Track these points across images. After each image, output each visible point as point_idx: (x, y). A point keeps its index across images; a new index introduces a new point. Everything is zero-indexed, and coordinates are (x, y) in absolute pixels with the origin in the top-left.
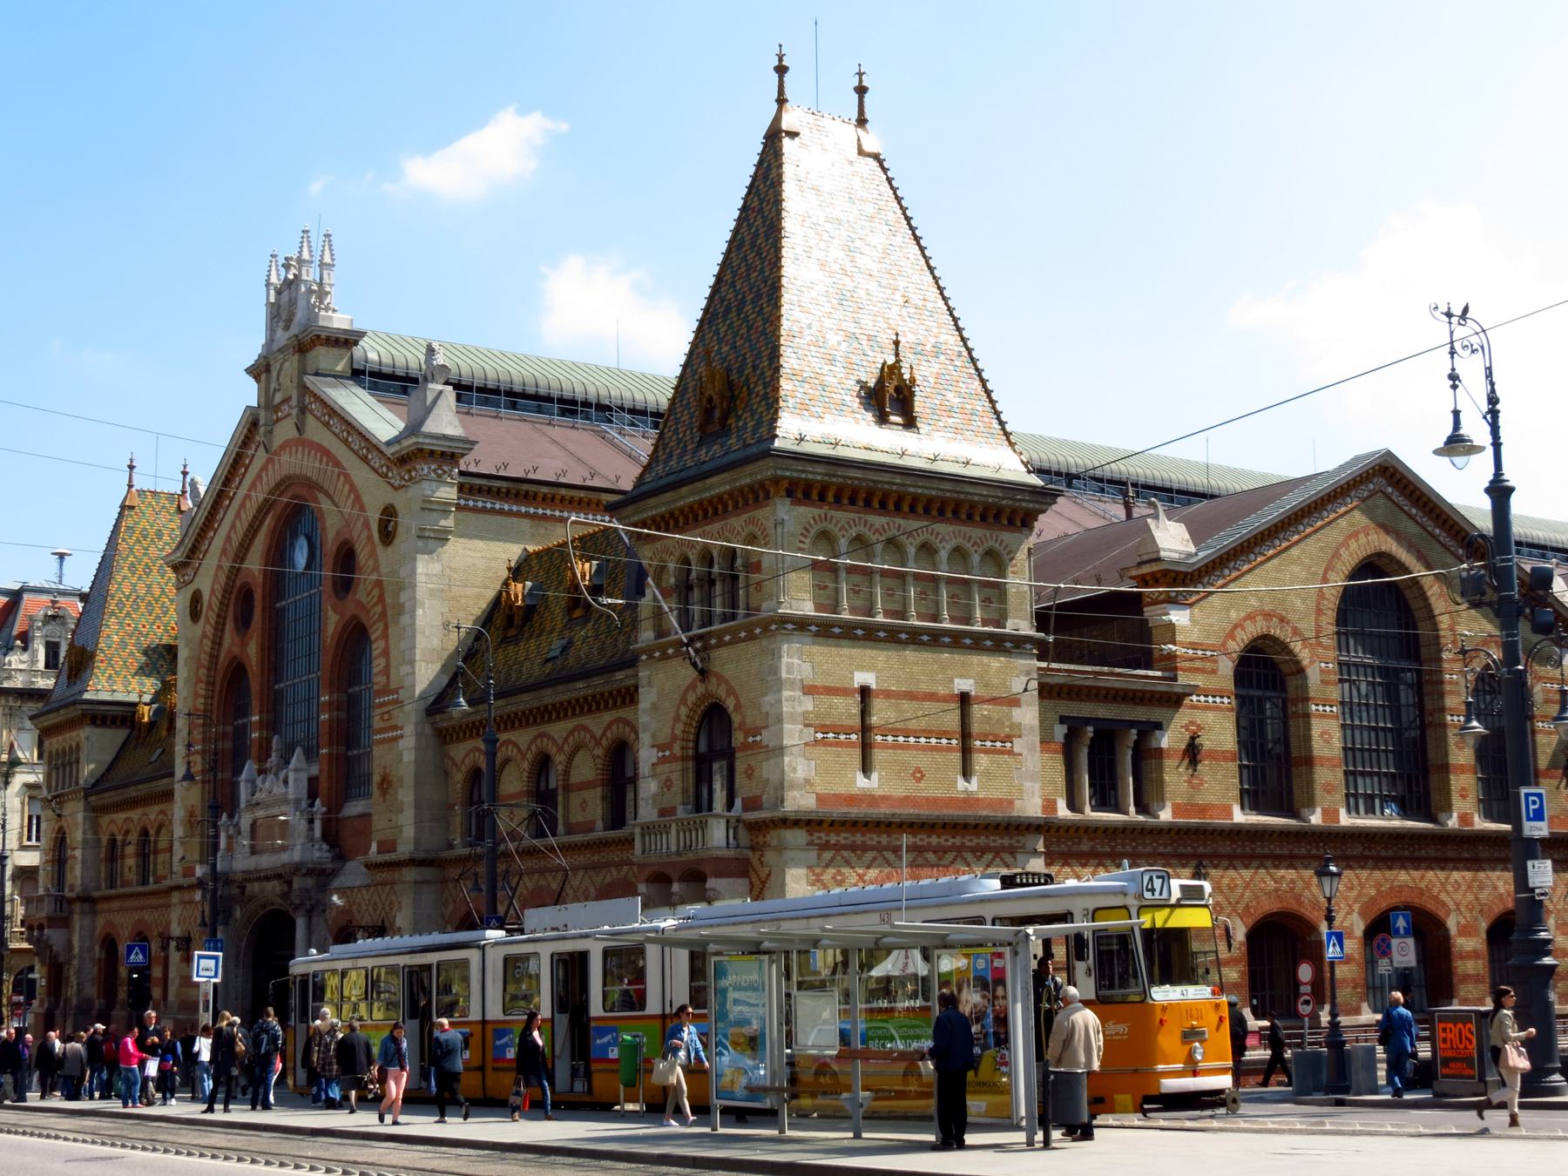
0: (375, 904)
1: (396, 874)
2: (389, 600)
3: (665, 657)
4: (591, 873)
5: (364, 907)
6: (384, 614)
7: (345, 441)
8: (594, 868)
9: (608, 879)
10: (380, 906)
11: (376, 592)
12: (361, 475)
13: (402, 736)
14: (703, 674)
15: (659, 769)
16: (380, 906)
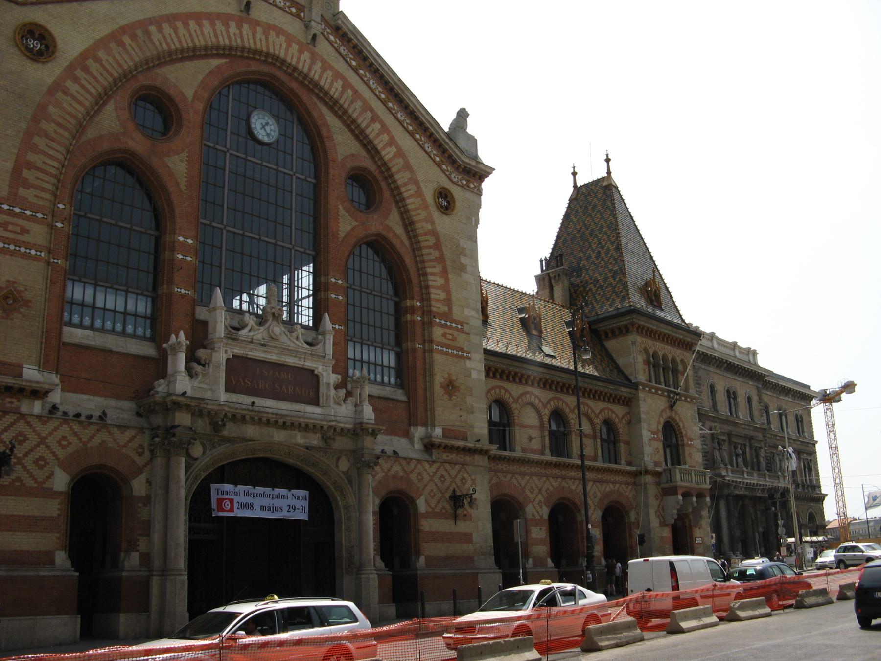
0: (442, 476)
1: (468, 459)
2: (448, 254)
3: (656, 393)
4: (597, 484)
5: (426, 478)
6: (441, 259)
7: (384, 103)
8: (599, 482)
9: (608, 489)
10: (449, 480)
11: (432, 241)
12: (406, 142)
13: (470, 359)
14: (671, 407)
15: (652, 442)
16: (449, 480)
